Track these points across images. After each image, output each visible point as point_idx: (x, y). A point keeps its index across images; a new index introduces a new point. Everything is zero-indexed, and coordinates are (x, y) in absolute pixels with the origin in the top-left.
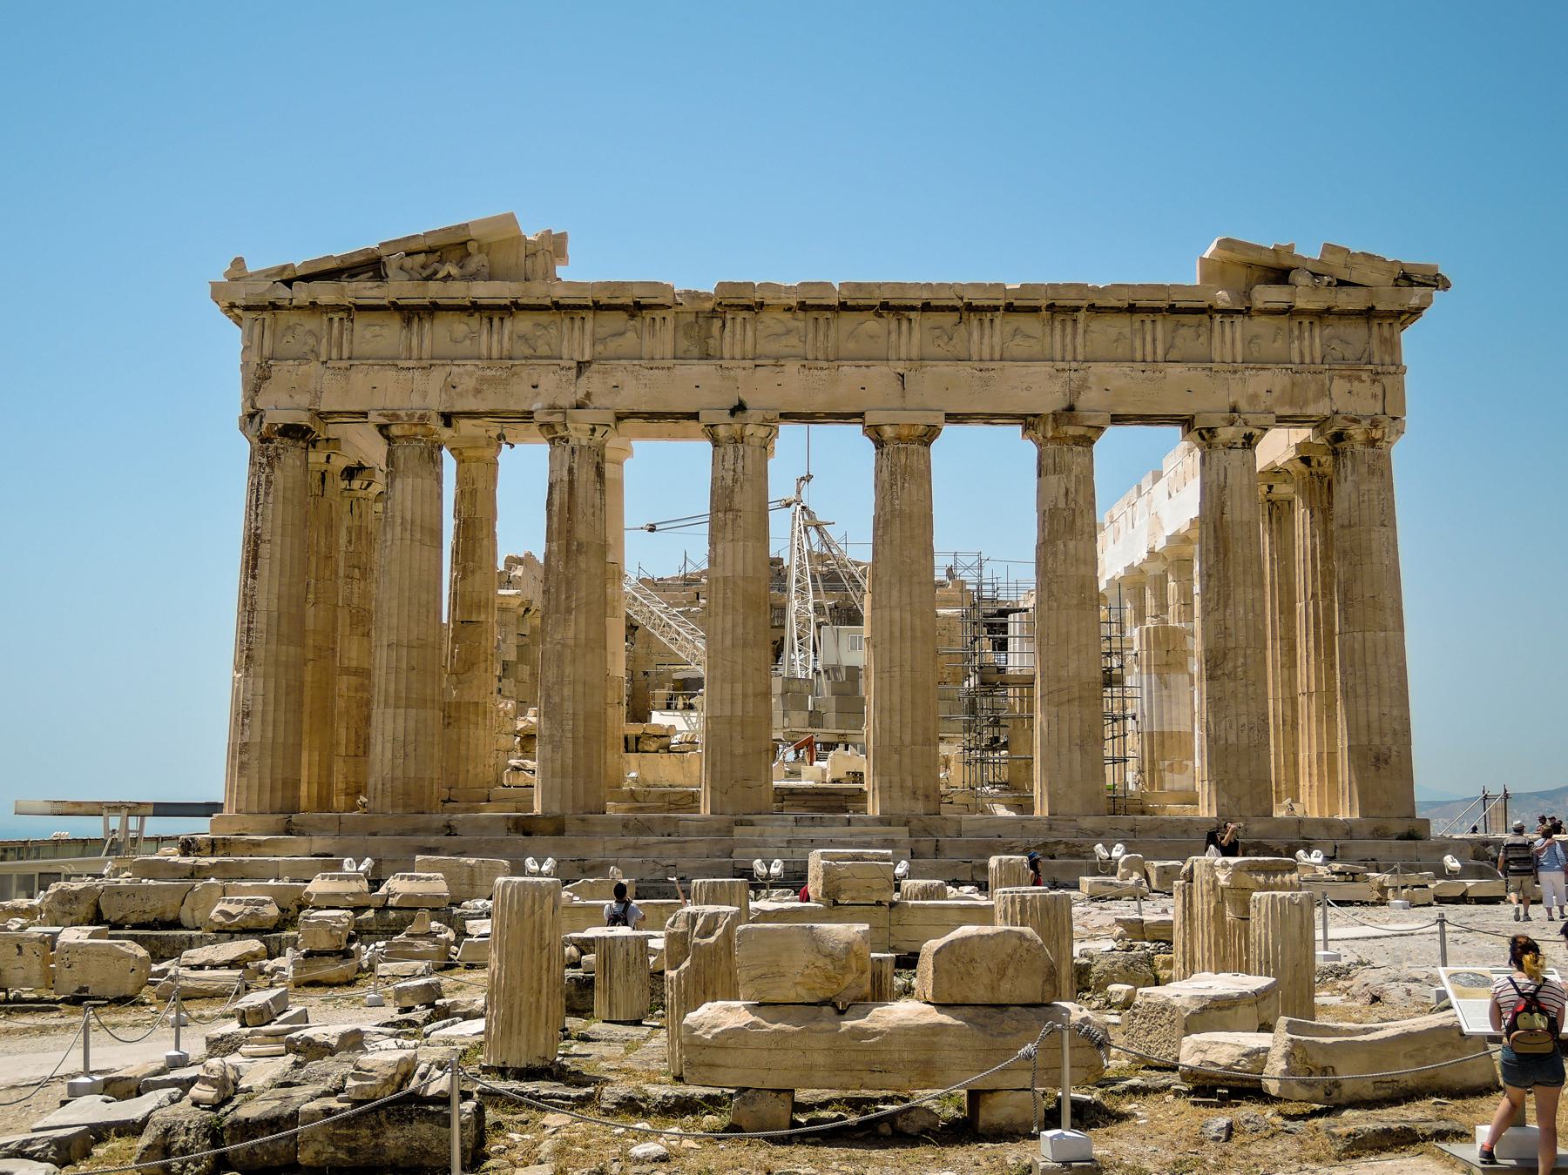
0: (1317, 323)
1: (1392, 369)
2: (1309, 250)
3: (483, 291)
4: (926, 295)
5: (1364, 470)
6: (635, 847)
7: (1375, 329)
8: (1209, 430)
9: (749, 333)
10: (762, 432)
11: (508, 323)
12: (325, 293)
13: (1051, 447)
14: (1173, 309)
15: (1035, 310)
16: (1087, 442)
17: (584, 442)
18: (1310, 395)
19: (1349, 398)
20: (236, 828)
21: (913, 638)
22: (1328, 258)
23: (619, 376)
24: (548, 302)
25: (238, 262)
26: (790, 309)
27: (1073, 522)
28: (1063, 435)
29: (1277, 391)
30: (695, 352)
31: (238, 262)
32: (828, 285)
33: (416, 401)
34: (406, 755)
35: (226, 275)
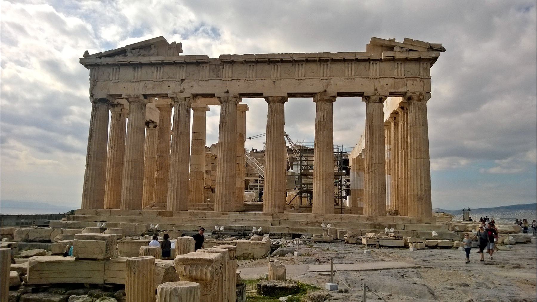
1: (427, 77)
2: (400, 40)
5: (417, 109)
6: (191, 221)
7: (422, 65)
8: (369, 97)
9: (230, 70)
10: (234, 99)
11: (162, 69)
12: (110, 60)
13: (320, 103)
14: (357, 60)
15: (314, 61)
16: (331, 100)
17: (183, 103)
18: (400, 85)
19: (412, 87)
20: (82, 213)
21: (276, 160)
22: (406, 42)
23: (193, 83)
24: (172, 61)
25: (87, 52)
26: (242, 63)
28: (325, 100)
29: (390, 84)
30: (215, 76)
31: (87, 52)
33: (136, 93)
34: (130, 193)
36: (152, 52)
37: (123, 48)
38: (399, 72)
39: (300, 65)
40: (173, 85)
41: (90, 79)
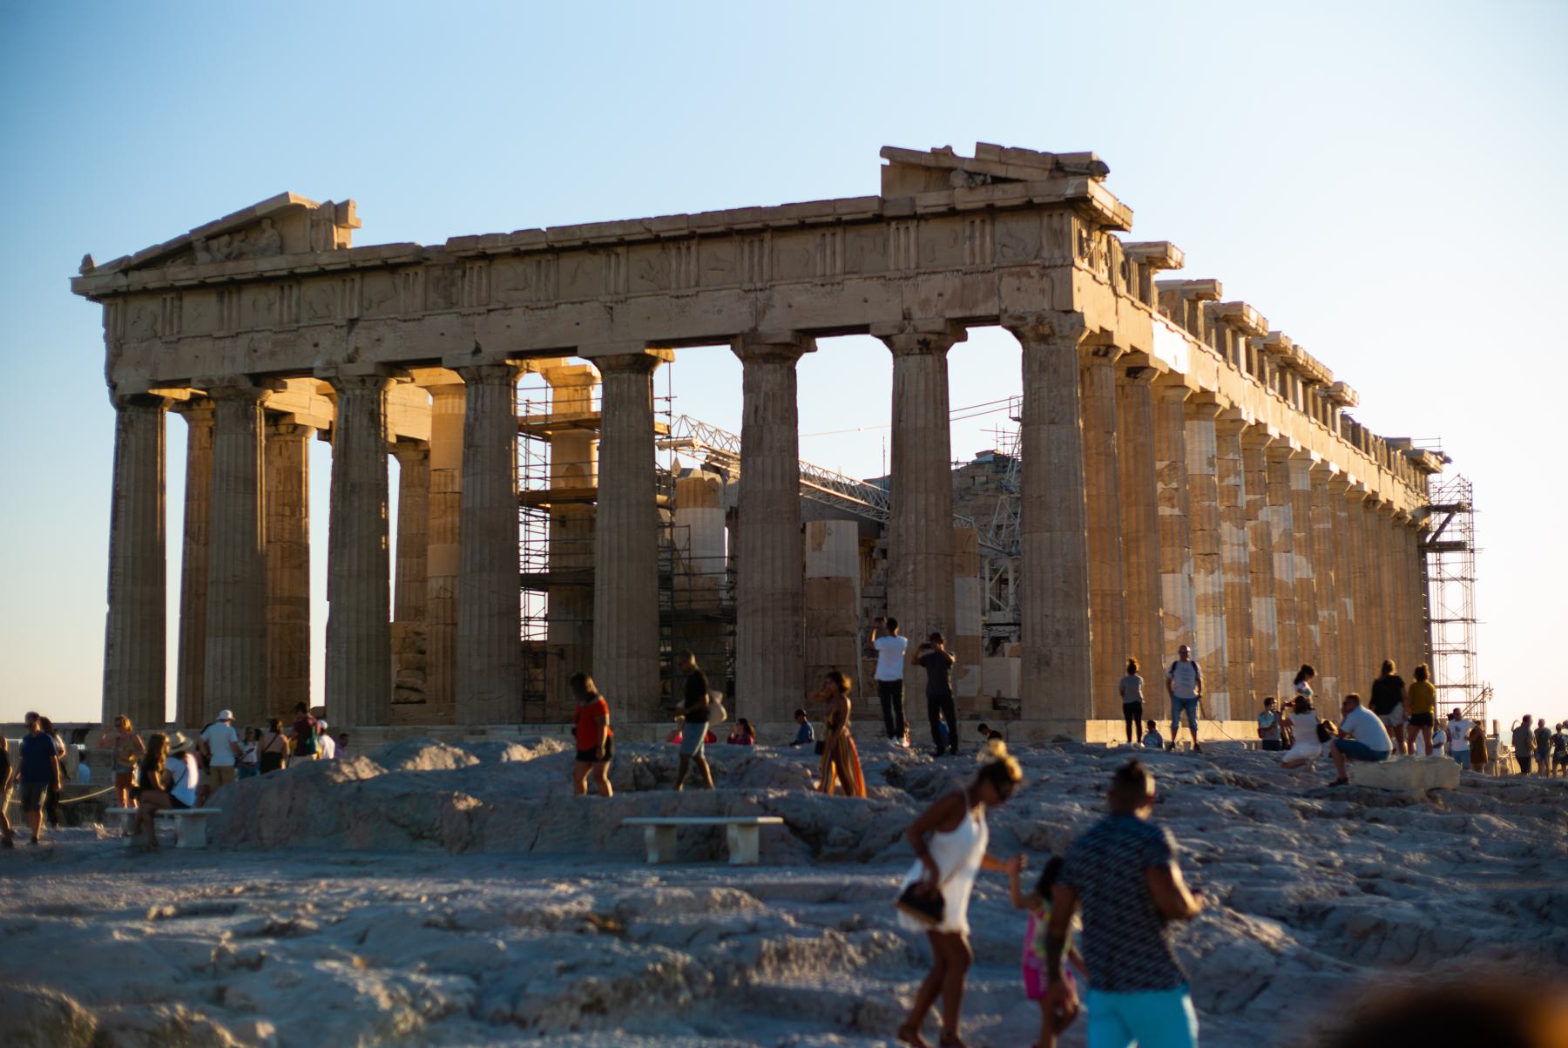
0: (988, 221)
1: (1059, 262)
2: (966, 150)
3: (267, 265)
4: (619, 232)
7: (1045, 220)
9: (484, 281)
11: (295, 291)
12: (150, 278)
17: (358, 392)
22: (983, 156)
24: (316, 269)
27: (761, 439)
29: (947, 296)
30: (441, 301)
32: (539, 230)
33: (227, 371)
34: (224, 678)
35: (82, 271)
36: (263, 242)
37: (183, 238)
38: (977, 249)
39: (684, 250)
40: (326, 339)
41: (106, 337)
